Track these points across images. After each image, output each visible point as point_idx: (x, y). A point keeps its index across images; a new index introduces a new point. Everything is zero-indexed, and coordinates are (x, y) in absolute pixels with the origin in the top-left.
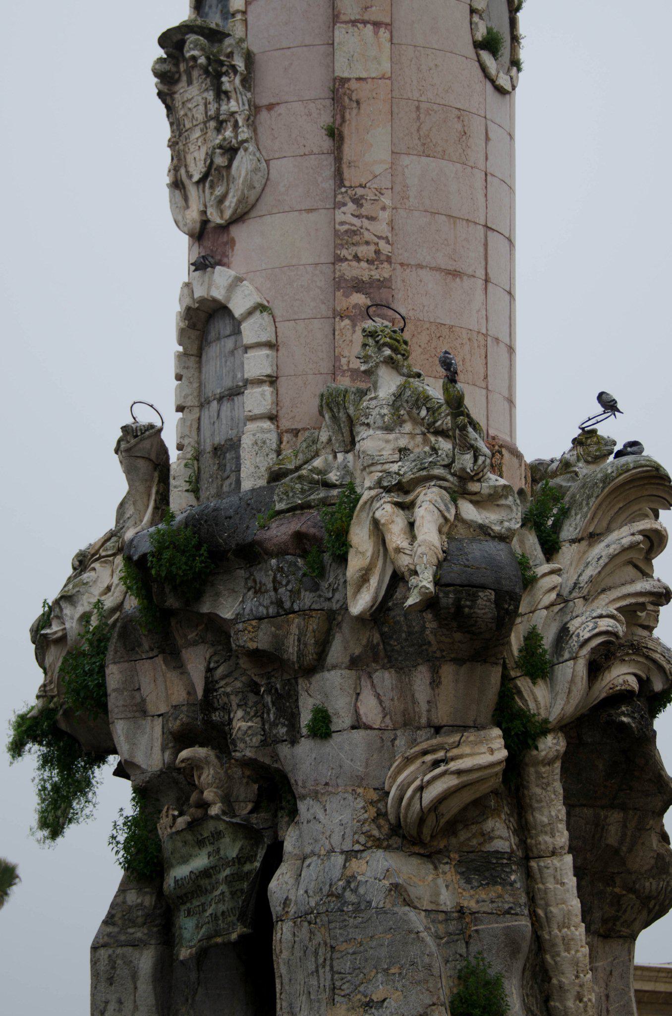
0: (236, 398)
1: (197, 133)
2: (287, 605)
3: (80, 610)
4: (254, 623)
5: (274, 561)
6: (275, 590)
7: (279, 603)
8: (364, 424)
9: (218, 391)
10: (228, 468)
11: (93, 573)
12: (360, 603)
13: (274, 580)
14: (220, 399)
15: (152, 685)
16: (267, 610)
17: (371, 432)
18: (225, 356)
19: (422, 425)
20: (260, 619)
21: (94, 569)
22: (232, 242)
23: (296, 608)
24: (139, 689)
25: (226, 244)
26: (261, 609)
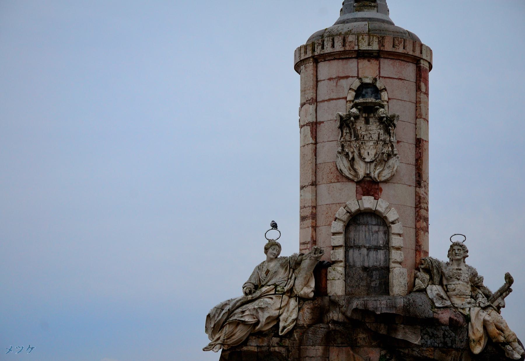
0: (379, 251)
1: (371, 143)
2: (450, 345)
3: (266, 315)
4: (432, 349)
5: (443, 327)
6: (444, 338)
7: (445, 343)
8: (457, 278)
9: (368, 245)
10: (374, 276)
11: (270, 300)
12: (477, 350)
13: (444, 334)
14: (369, 249)
15: (336, 357)
16: (439, 344)
17: (460, 282)
18: (372, 232)
19: (473, 283)
20: (435, 348)
21: (272, 298)
22: (381, 190)
23: (454, 346)
24: (328, 358)
25: (377, 189)
26: (436, 344)
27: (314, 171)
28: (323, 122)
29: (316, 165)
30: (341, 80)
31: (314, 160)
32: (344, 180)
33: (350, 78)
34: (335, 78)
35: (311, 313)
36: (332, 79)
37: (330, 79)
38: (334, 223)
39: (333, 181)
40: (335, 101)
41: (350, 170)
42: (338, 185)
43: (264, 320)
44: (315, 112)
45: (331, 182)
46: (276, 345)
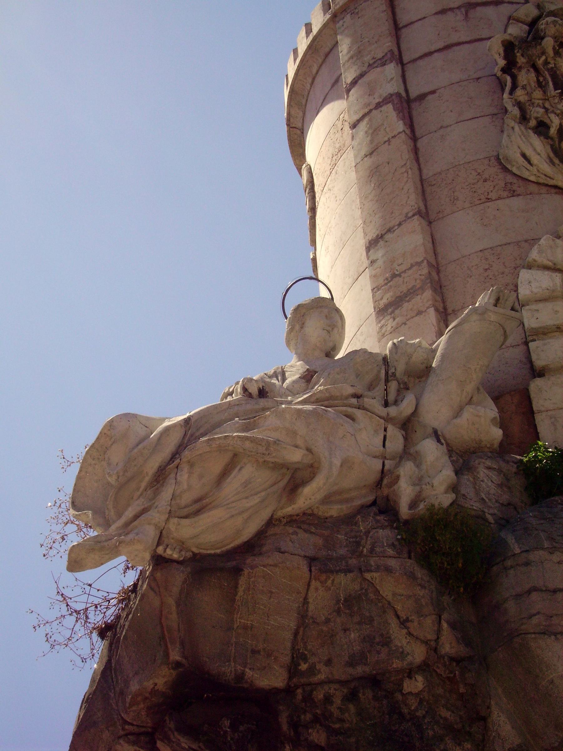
27: (420, 190)
28: (433, 92)
29: (422, 181)
30: (479, 9)
31: (417, 172)
32: (533, 188)
33: (505, 5)
34: (459, 8)
35: (500, 486)
36: (451, 9)
37: (443, 12)
38: (524, 275)
39: (493, 195)
40: (467, 46)
41: (551, 161)
42: (516, 202)
43: (337, 462)
44: (400, 80)
45: (489, 200)
46: (390, 552)
